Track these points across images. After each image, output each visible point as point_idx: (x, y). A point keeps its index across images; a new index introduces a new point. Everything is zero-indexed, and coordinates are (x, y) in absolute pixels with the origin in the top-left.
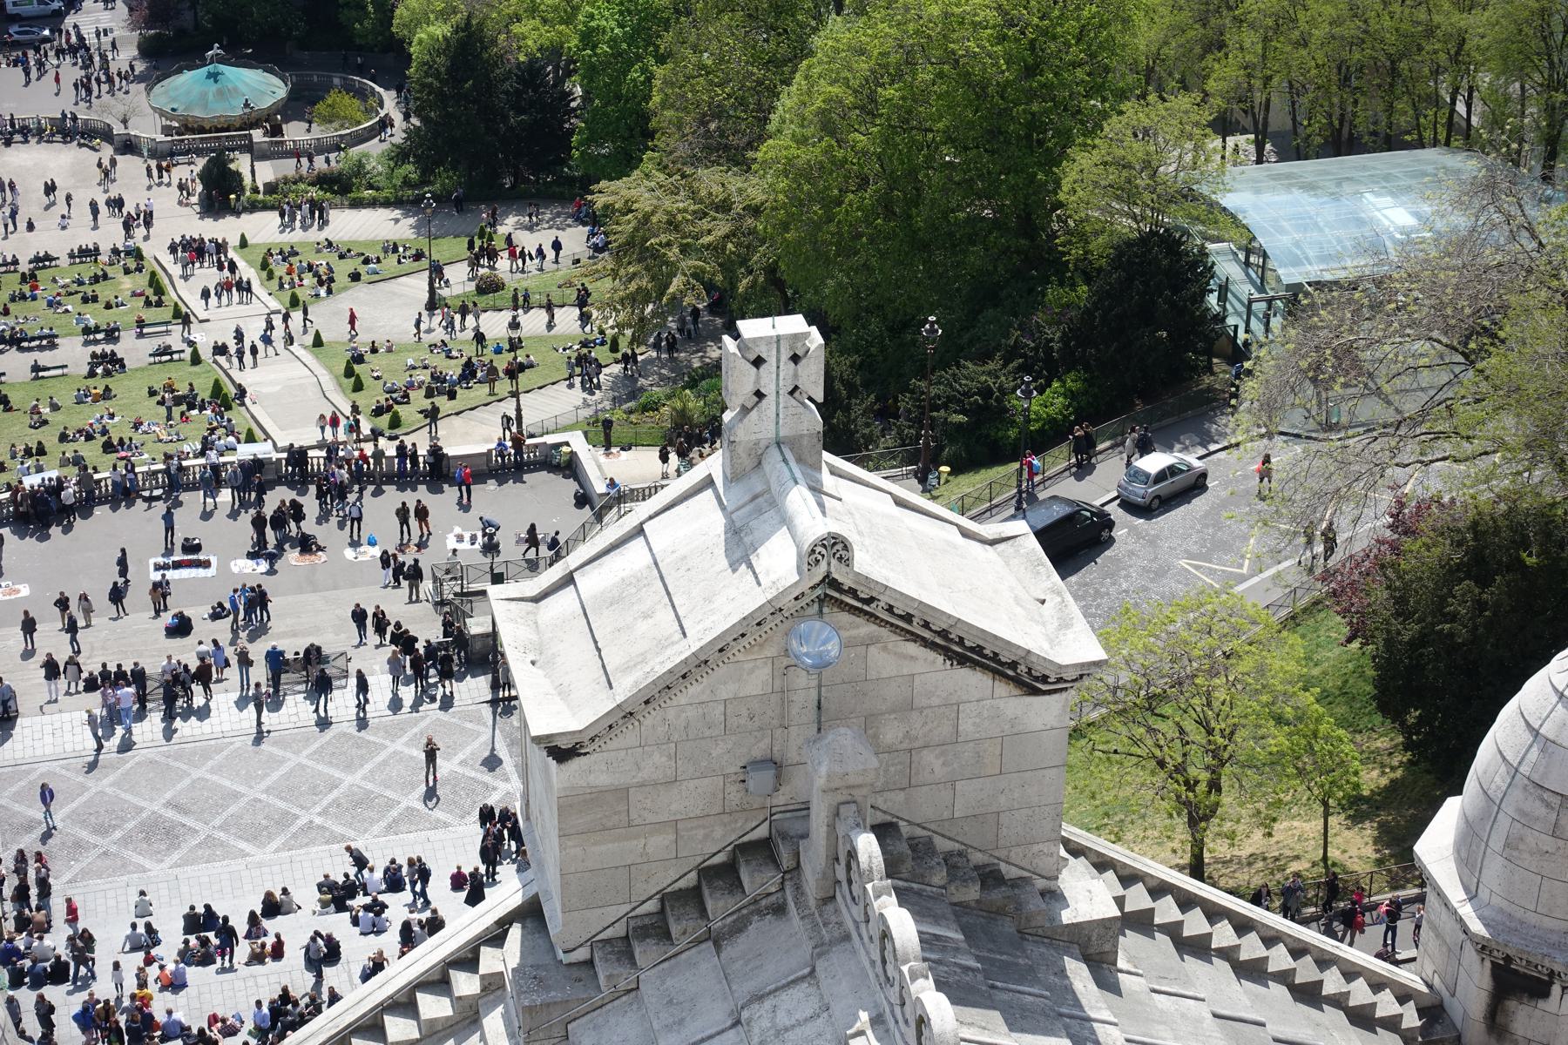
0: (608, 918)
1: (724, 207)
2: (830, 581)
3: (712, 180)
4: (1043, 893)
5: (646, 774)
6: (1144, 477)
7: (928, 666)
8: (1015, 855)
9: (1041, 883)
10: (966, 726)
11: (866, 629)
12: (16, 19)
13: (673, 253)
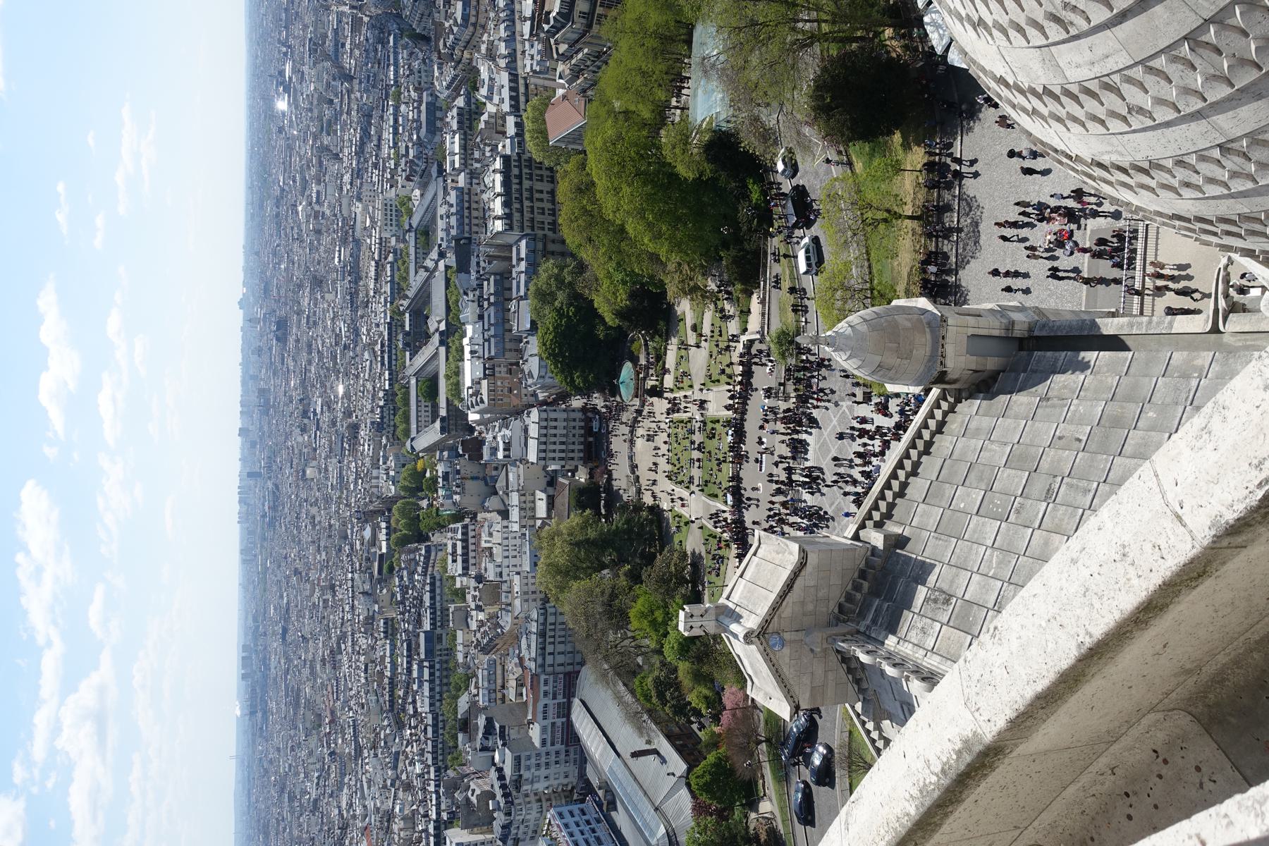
0: (851, 689)
1: (680, 264)
2: (758, 636)
3: (671, 267)
4: (873, 554)
5: (809, 683)
6: (784, 171)
7: (790, 598)
8: (858, 562)
9: (869, 553)
10: (812, 583)
11: (776, 618)
12: (600, 429)
13: (692, 283)
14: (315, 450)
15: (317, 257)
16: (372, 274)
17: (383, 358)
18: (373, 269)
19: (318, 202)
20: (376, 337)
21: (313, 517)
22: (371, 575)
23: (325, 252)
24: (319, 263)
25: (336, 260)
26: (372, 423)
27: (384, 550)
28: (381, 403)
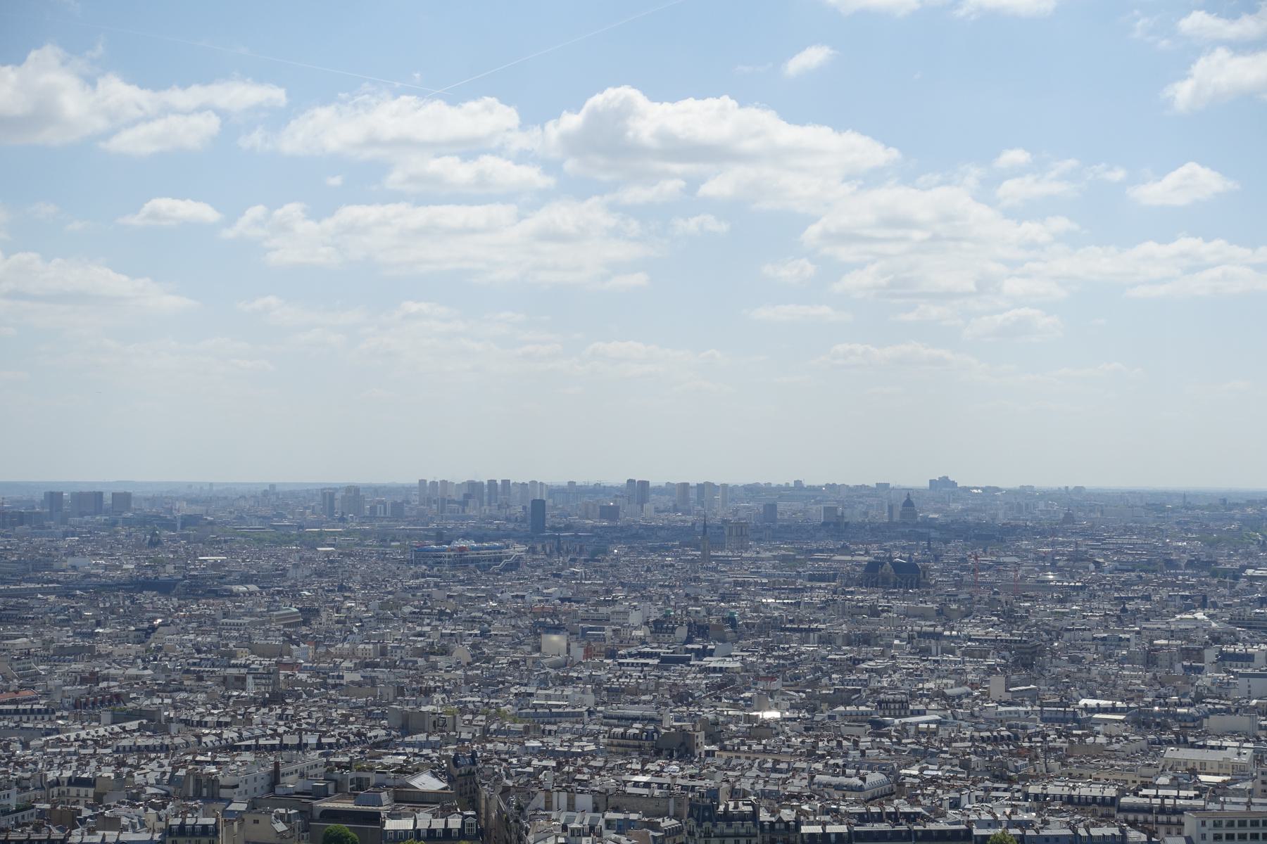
14: (612, 654)
15: (1090, 656)
16: (1084, 791)
17: (879, 818)
18: (1096, 791)
19: (1224, 657)
20: (927, 802)
21: (445, 652)
22: (321, 794)
23: (1105, 676)
24: (1073, 660)
25: (1092, 703)
26: (714, 794)
27: (391, 825)
28: (764, 816)
